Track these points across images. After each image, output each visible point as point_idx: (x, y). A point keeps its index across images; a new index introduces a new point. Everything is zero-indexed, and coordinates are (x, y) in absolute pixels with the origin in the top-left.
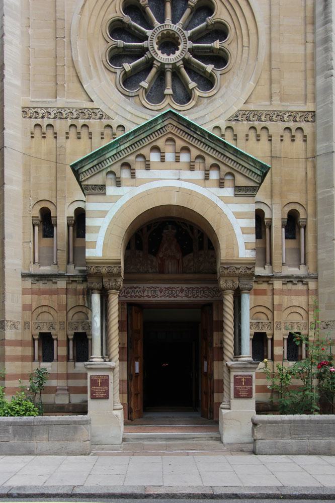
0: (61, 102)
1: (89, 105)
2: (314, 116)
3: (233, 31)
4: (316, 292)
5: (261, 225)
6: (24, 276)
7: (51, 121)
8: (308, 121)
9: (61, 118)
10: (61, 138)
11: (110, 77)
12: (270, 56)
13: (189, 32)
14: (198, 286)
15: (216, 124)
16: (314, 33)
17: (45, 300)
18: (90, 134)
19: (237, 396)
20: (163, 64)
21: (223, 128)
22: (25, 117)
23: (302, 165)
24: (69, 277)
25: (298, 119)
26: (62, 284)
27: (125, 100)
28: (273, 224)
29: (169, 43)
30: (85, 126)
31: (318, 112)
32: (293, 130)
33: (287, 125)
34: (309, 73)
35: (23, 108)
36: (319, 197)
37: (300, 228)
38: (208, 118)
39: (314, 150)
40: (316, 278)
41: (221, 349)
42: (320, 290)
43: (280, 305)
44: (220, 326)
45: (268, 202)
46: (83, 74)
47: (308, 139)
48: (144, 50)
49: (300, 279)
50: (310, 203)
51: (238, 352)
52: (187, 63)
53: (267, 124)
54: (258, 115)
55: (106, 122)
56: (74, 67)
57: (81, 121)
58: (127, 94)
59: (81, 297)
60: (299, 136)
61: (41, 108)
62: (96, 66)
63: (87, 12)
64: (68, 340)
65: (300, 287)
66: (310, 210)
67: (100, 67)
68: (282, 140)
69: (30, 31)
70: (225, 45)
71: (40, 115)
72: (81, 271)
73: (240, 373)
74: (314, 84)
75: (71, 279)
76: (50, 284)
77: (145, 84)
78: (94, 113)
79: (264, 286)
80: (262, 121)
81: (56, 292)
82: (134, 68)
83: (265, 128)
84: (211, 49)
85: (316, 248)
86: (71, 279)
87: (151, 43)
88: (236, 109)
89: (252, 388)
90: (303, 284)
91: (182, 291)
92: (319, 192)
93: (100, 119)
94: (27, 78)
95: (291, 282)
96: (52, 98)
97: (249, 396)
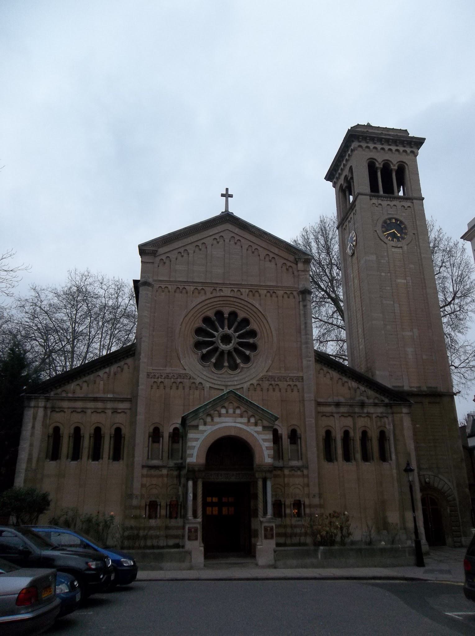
0: (168, 370)
1: (183, 372)
2: (302, 379)
3: (260, 334)
4: (307, 476)
5: (277, 438)
6: (143, 467)
7: (163, 380)
8: (300, 382)
13: (237, 334)
17: (154, 481)
18: (184, 387)
19: (266, 537)
21: (255, 385)
22: (149, 378)
24: (169, 467)
25: (294, 380)
26: (165, 472)
28: (283, 437)
29: (226, 339)
30: (181, 382)
31: (304, 377)
32: (292, 386)
33: (289, 383)
35: (147, 373)
36: (307, 423)
38: (247, 379)
39: (303, 397)
40: (307, 468)
41: (256, 510)
44: (256, 496)
45: (280, 425)
47: (300, 391)
48: (212, 343)
49: (299, 468)
51: (265, 513)
52: (236, 350)
53: (278, 383)
55: (192, 381)
57: (179, 380)
58: (204, 365)
59: (175, 479)
61: (158, 373)
63: (184, 325)
64: (167, 505)
65: (299, 473)
68: (286, 391)
70: (256, 341)
71: (157, 377)
72: (175, 464)
73: (267, 524)
74: (302, 363)
75: (170, 469)
76: (157, 471)
77: (213, 360)
78: (185, 376)
79: (279, 472)
80: (275, 381)
81: (162, 476)
82: (208, 352)
83: (277, 385)
84: (248, 343)
86: (170, 469)
88: (262, 375)
89: (273, 533)
90: (300, 471)
92: (307, 420)
95: (294, 470)
97: (272, 537)
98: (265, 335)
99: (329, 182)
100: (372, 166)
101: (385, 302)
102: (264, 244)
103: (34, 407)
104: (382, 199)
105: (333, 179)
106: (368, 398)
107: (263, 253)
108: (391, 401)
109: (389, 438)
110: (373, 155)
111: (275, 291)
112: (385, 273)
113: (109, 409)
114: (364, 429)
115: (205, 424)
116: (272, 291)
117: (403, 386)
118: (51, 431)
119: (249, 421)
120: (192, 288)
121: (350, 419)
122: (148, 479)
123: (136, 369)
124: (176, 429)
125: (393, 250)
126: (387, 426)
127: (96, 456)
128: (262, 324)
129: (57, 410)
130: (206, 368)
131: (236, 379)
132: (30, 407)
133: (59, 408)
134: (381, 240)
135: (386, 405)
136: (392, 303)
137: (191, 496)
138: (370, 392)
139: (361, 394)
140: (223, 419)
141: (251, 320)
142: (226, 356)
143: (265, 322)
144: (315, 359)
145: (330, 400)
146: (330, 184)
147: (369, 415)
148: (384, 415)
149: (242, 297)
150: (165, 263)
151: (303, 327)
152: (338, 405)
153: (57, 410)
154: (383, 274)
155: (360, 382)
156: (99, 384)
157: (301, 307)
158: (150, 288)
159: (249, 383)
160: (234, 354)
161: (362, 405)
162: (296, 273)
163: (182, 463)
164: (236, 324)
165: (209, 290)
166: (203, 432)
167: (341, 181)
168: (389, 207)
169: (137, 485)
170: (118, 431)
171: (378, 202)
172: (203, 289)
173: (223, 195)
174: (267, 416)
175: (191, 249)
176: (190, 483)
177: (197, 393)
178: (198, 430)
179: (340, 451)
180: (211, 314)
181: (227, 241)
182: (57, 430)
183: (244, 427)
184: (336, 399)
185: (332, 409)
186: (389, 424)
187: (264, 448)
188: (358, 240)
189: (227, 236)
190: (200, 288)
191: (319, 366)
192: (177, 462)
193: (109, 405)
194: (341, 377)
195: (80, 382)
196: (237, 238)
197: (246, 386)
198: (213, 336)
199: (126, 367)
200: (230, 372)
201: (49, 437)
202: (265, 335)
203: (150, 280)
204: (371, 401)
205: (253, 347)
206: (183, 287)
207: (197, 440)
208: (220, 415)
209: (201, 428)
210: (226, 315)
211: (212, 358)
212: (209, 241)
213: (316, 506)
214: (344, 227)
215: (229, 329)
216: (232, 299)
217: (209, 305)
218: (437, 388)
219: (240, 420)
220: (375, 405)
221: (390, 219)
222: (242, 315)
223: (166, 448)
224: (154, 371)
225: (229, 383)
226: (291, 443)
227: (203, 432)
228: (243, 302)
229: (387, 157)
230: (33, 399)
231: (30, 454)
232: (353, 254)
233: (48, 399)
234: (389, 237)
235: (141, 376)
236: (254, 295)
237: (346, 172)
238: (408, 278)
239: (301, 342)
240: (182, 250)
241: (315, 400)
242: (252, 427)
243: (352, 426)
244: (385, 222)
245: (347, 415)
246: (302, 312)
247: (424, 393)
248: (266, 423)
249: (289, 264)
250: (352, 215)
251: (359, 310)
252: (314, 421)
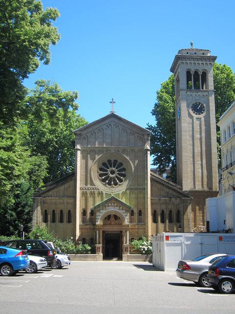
19: (125, 251)
20: (111, 178)
29: (113, 172)
51: (126, 243)
100: (188, 73)
107: (129, 131)
110: (189, 67)
115: (103, 209)
127: (61, 221)
137: (98, 236)
140: (110, 208)
166: (102, 212)
170: (69, 211)
173: (111, 102)
175: (96, 131)
181: (113, 126)
182: (46, 211)
183: (118, 211)
200: (114, 186)
209: (101, 211)
212: (104, 127)
219: (116, 208)
221: (196, 103)
227: (102, 212)
229: (197, 67)
240: (92, 132)
244: (193, 105)
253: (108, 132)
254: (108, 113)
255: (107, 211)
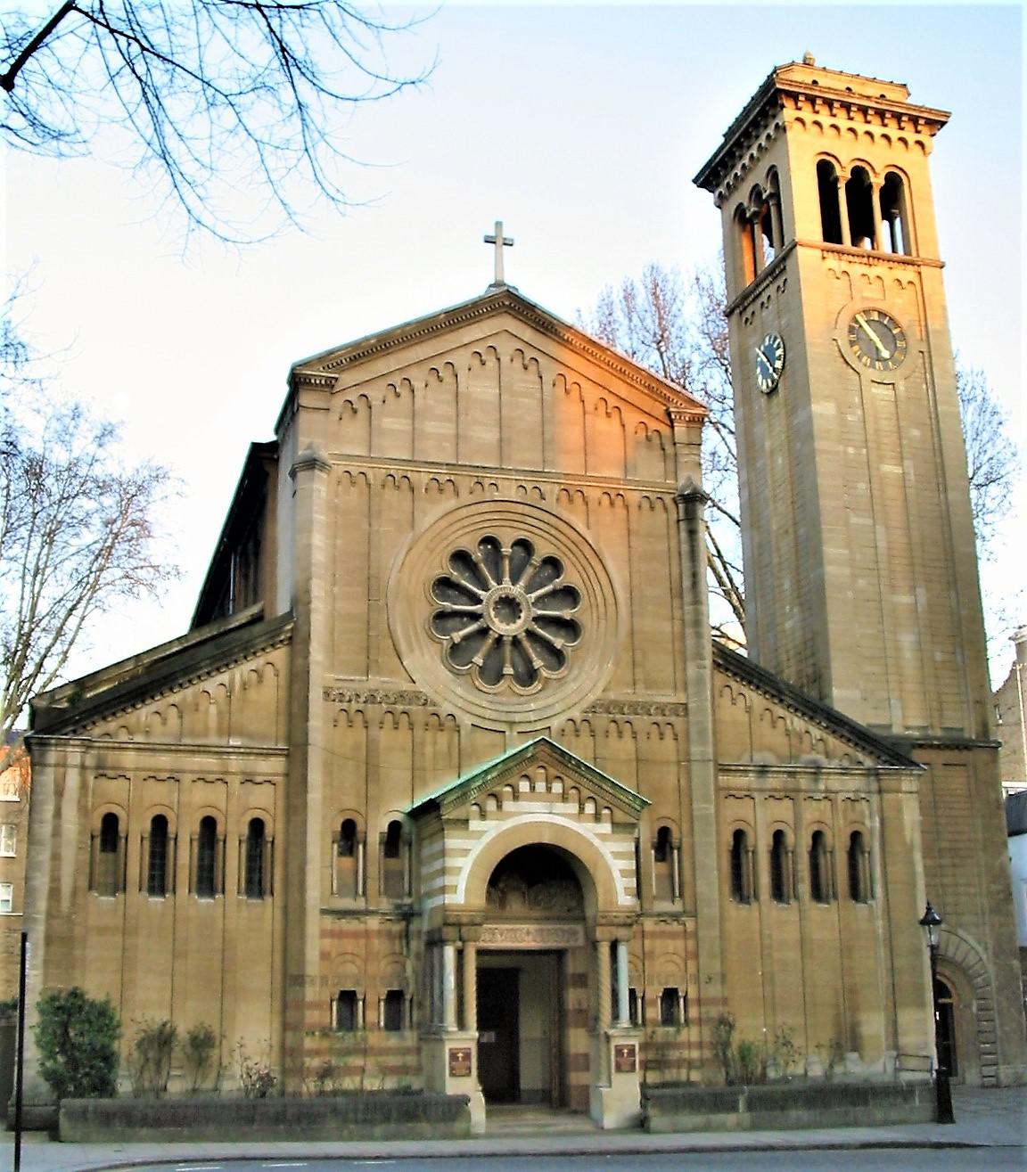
0: (374, 681)
4: (695, 935)
7: (361, 706)
9: (373, 703)
10: (374, 730)
11: (434, 648)
12: (632, 633)
14: (550, 927)
15: (568, 715)
16: (682, 608)
17: (349, 945)
19: (619, 1069)
22: (326, 700)
23: (673, 769)
25: (667, 713)
26: (373, 923)
27: (453, 681)
29: (510, 606)
31: (690, 706)
32: (662, 726)
33: (654, 719)
34: (678, 658)
35: (325, 687)
36: (696, 813)
37: (672, 849)
38: (558, 708)
39: (688, 753)
40: (695, 915)
42: (701, 933)
43: (652, 952)
46: (403, 648)
48: (475, 617)
49: (675, 917)
50: (685, 818)
51: (616, 1016)
52: (530, 634)
54: (619, 706)
55: (431, 709)
56: (392, 637)
57: (400, 707)
59: (397, 942)
60: (668, 731)
62: (416, 634)
63: (406, 569)
65: (675, 927)
66: (685, 827)
67: (423, 637)
69: (336, 589)
71: (348, 698)
72: (398, 907)
74: (685, 670)
78: (416, 697)
81: (367, 934)
82: (466, 638)
85: (694, 876)
87: (487, 608)
88: (592, 698)
90: (679, 924)
91: (528, 933)
92: (695, 806)
93: (424, 705)
94: (332, 649)
96: (362, 675)
98: (600, 598)
99: (704, 191)
100: (825, 171)
101: (854, 520)
102: (593, 372)
103: (56, 765)
104: (851, 258)
105: (718, 186)
106: (828, 755)
107: (592, 394)
108: (879, 764)
109: (871, 848)
111: (621, 492)
112: (856, 447)
113: (233, 773)
114: (816, 828)
115: (483, 815)
116: (614, 497)
117: (890, 726)
118: (97, 824)
119: (582, 809)
120: (425, 478)
121: (787, 803)
122: (336, 941)
123: (298, 679)
124: (395, 826)
125: (874, 390)
126: (867, 822)
128: (591, 572)
129: (111, 773)
130: (462, 679)
131: (533, 706)
132: (44, 765)
133: (113, 768)
134: (847, 363)
135: (870, 773)
136: (869, 522)
138: (832, 741)
139: (813, 748)
140: (523, 805)
141: (565, 562)
142: (508, 649)
143: (598, 568)
144: (714, 661)
145: (745, 760)
146: (707, 197)
147: (829, 796)
148: (863, 796)
149: (542, 504)
150: (355, 411)
151: (687, 583)
152: (763, 770)
153: (111, 773)
154: (851, 450)
155: (811, 718)
156: (207, 712)
157: (684, 535)
158: (324, 475)
159: (563, 717)
160: (526, 644)
161: (817, 771)
162: (669, 449)
163: (411, 906)
164: (529, 571)
165: (465, 483)
167: (742, 196)
168: (865, 280)
169: (313, 950)
170: (257, 826)
171: (840, 266)
172: (450, 480)
174: (624, 799)
175: (418, 377)
176: (450, 953)
177: (443, 739)
178: (468, 828)
179: (765, 879)
180: (469, 544)
181: (505, 359)
184: (759, 758)
185: (750, 780)
186: (871, 817)
187: (616, 874)
188: (788, 357)
189: (506, 348)
190: (443, 479)
191: (721, 678)
192: (399, 901)
193: (235, 763)
194: (771, 706)
195: (159, 704)
196: (530, 353)
197: (555, 724)
198: (478, 601)
199: (269, 671)
200: (518, 689)
201: (93, 837)
202: (600, 598)
203: (324, 454)
204: (835, 763)
205: (570, 628)
206: (401, 473)
207: (466, 852)
208: (516, 796)
209: (475, 825)
210: (506, 550)
211: (477, 651)
212: (462, 359)
213: (714, 1001)
214: (748, 314)
215: (514, 581)
216: (520, 508)
217: (466, 522)
218: (962, 730)
220: (845, 772)
222: (543, 549)
223: (373, 870)
224: (340, 684)
225: (517, 718)
226: (657, 860)
228: (546, 517)
230: (50, 745)
231: (55, 879)
232: (772, 392)
233: (88, 745)
234: (865, 358)
235: (312, 696)
236: (571, 501)
237: (758, 177)
238: (907, 463)
239: (683, 620)
240: (397, 380)
241: (715, 761)
242: (591, 825)
243: (791, 822)
245: (782, 794)
246: (685, 548)
247: (935, 742)
248: (620, 816)
249: (653, 425)
250: (772, 291)
251: (787, 532)
252: (713, 811)
253: (480, 388)
254: (474, 288)
255: (508, 824)
